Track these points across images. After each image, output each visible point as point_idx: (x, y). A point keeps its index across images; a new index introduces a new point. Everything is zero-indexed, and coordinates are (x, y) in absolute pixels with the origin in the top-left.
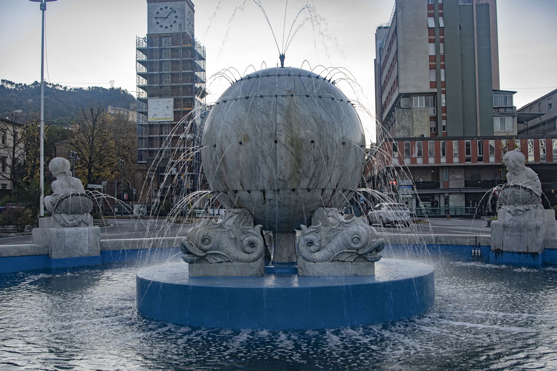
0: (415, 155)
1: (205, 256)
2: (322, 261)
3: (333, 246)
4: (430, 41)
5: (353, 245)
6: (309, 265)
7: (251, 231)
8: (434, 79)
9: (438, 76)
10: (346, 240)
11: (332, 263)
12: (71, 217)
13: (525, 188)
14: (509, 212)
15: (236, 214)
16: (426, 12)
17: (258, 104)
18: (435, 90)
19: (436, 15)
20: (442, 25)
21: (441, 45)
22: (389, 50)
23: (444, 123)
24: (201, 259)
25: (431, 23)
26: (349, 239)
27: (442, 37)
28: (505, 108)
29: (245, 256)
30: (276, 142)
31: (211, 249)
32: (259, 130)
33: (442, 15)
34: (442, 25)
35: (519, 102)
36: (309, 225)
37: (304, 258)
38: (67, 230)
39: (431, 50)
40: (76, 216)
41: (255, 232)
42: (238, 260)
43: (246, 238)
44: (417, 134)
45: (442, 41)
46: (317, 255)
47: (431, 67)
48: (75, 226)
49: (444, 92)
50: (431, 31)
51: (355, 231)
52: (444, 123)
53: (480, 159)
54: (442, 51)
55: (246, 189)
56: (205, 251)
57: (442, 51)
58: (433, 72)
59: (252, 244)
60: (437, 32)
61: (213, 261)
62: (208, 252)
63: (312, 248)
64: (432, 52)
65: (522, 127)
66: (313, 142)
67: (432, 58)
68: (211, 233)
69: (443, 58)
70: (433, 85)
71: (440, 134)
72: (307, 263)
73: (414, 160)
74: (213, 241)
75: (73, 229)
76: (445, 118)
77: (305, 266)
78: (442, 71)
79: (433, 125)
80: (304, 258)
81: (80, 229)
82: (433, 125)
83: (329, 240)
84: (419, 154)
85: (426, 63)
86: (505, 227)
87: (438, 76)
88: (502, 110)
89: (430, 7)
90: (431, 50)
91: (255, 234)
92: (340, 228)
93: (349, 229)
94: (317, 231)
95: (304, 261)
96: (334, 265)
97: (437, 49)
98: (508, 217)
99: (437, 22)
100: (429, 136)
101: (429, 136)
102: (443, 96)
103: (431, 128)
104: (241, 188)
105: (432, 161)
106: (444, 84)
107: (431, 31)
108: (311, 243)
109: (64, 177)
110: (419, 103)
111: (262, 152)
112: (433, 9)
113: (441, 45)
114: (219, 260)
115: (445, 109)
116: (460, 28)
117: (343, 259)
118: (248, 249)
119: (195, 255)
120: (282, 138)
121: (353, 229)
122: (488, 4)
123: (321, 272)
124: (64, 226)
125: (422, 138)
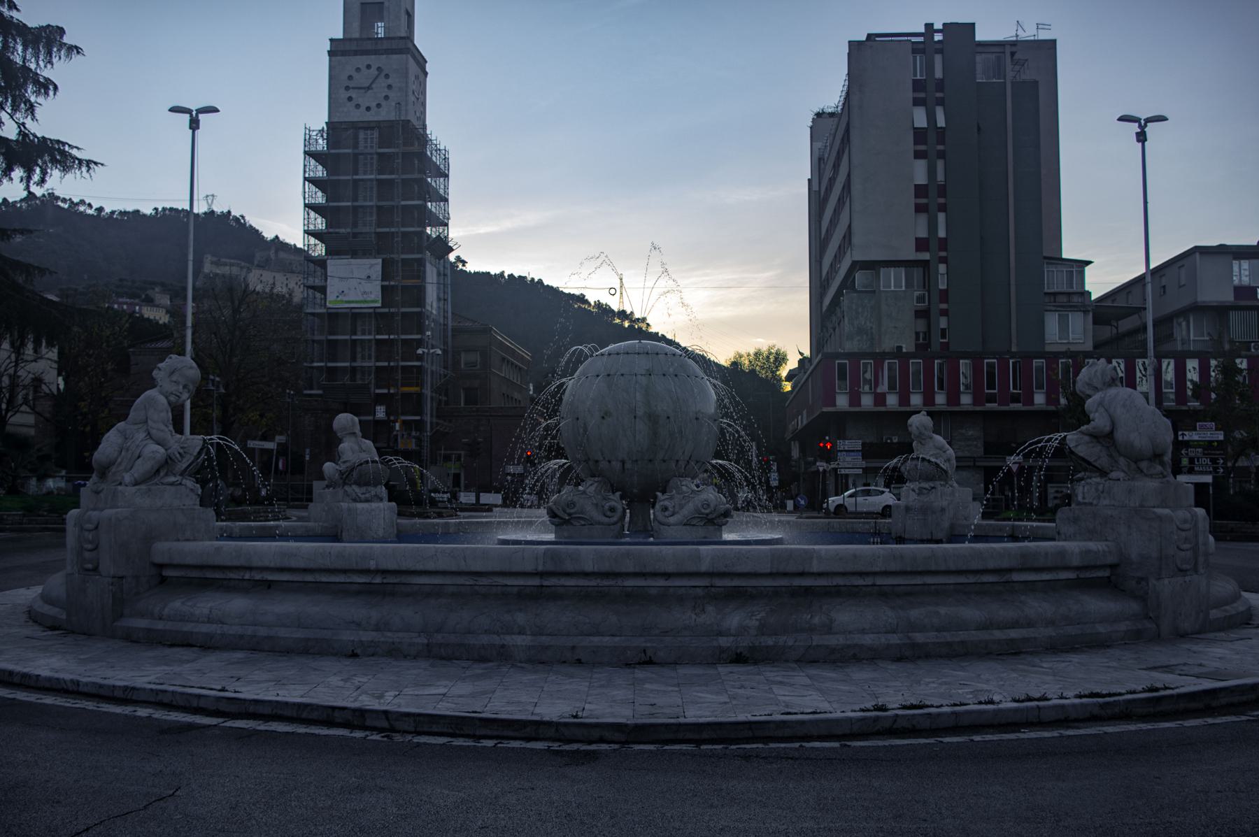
0: (883, 387)
3: (685, 512)
4: (918, 155)
8: (923, 233)
9: (933, 226)
12: (364, 489)
16: (910, 95)
18: (926, 256)
20: (941, 122)
22: (836, 167)
23: (943, 322)
25: (920, 119)
27: (940, 147)
28: (1069, 294)
29: (606, 520)
33: (941, 102)
34: (941, 122)
35: (1098, 283)
36: (664, 492)
38: (360, 506)
40: (370, 488)
42: (599, 523)
44: (888, 345)
45: (941, 155)
46: (672, 520)
47: (919, 209)
48: (367, 501)
49: (944, 260)
50: (920, 135)
52: (943, 322)
53: (1016, 399)
54: (940, 177)
56: (569, 515)
57: (940, 177)
58: (923, 219)
59: (612, 509)
64: (921, 178)
65: (1107, 332)
67: (920, 191)
68: (576, 499)
69: (942, 191)
70: (921, 245)
71: (935, 347)
73: (880, 399)
75: (365, 505)
76: (944, 313)
78: (941, 217)
79: (921, 325)
80: (661, 523)
81: (374, 505)
82: (921, 325)
83: (682, 507)
84: (892, 387)
85: (911, 201)
87: (933, 226)
89: (917, 85)
94: (671, 498)
97: (932, 172)
99: (931, 117)
100: (912, 349)
101: (912, 349)
102: (942, 268)
103: (917, 334)
106: (943, 244)
107: (920, 135)
108: (665, 509)
109: (353, 439)
110: (893, 280)
115: (944, 296)
116: (979, 129)
118: (609, 513)
120: (640, 412)
121: (704, 496)
122: (1037, 82)
124: (355, 500)
125: (898, 353)
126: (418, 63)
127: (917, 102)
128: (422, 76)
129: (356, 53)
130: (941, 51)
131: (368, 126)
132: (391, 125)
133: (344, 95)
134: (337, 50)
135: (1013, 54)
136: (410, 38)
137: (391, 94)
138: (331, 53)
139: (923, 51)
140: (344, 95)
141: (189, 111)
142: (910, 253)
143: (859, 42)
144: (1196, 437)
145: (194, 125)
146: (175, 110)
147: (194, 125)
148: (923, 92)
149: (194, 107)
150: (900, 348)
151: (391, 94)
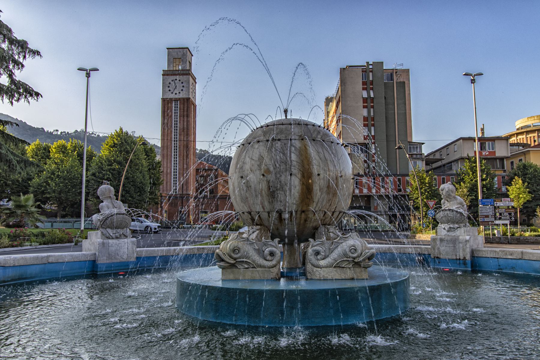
1: (235, 263)
2: (326, 267)
3: (334, 255)
4: (364, 107)
5: (351, 255)
6: (316, 270)
7: (271, 243)
10: (345, 250)
11: (335, 269)
13: (457, 212)
14: (444, 229)
15: (258, 230)
16: (361, 86)
17: (277, 145)
19: (368, 89)
20: (372, 96)
21: (372, 110)
24: (233, 266)
26: (347, 250)
27: (372, 104)
28: (417, 154)
30: (291, 175)
31: (240, 258)
32: (278, 165)
33: (372, 89)
34: (372, 96)
35: (425, 151)
36: (314, 237)
37: (313, 265)
39: (365, 112)
41: (274, 244)
42: (260, 266)
43: (267, 249)
45: (372, 107)
46: (322, 263)
49: (374, 143)
50: (365, 100)
51: (352, 244)
53: (400, 190)
54: (372, 114)
55: (266, 210)
56: (235, 259)
57: (372, 114)
59: (272, 254)
60: (369, 101)
61: (242, 267)
62: (238, 260)
63: (319, 257)
65: (429, 168)
66: (319, 175)
67: (365, 119)
68: (240, 245)
69: (373, 119)
72: (315, 269)
74: (242, 251)
77: (313, 271)
78: (373, 128)
80: (313, 265)
86: (442, 240)
88: (414, 156)
89: (364, 83)
90: (365, 112)
91: (277, 247)
92: (340, 241)
93: (347, 242)
94: (322, 244)
95: (312, 267)
96: (336, 271)
97: (369, 112)
98: (444, 232)
99: (369, 94)
104: (262, 210)
105: (365, 191)
107: (365, 100)
108: (317, 253)
111: (280, 182)
112: (366, 84)
113: (372, 110)
114: (246, 266)
117: (343, 266)
118: (269, 258)
119: (231, 264)
121: (351, 242)
122: (404, 82)
123: (326, 276)
126: (193, 79)
127: (364, 89)
128: (194, 83)
129: (172, 75)
130: (372, 72)
131: (176, 100)
132: (184, 99)
133: (168, 89)
134: (166, 74)
135: (396, 72)
136: (190, 70)
137: (184, 89)
138: (163, 75)
139: (366, 71)
140: (168, 89)
141: (87, 70)
142: (362, 140)
143: (344, 69)
144: (502, 205)
145: (88, 75)
146: (80, 69)
147: (88, 75)
148: (367, 85)
149: (88, 68)
150: (359, 173)
151: (184, 89)
